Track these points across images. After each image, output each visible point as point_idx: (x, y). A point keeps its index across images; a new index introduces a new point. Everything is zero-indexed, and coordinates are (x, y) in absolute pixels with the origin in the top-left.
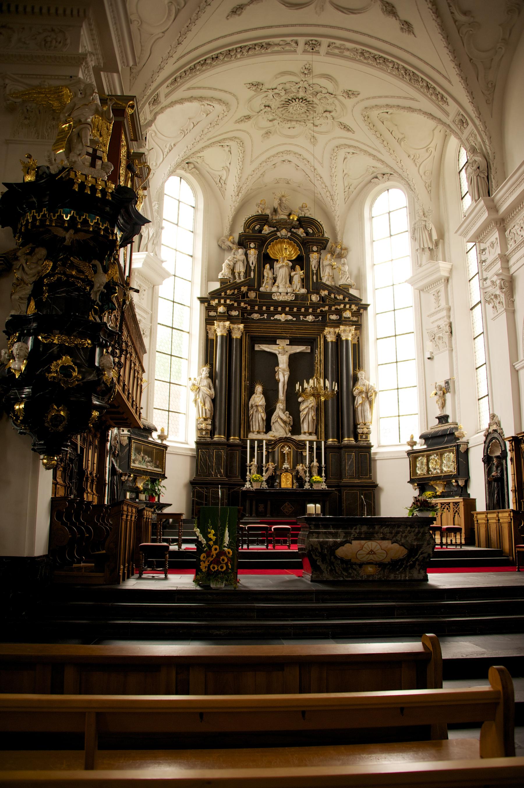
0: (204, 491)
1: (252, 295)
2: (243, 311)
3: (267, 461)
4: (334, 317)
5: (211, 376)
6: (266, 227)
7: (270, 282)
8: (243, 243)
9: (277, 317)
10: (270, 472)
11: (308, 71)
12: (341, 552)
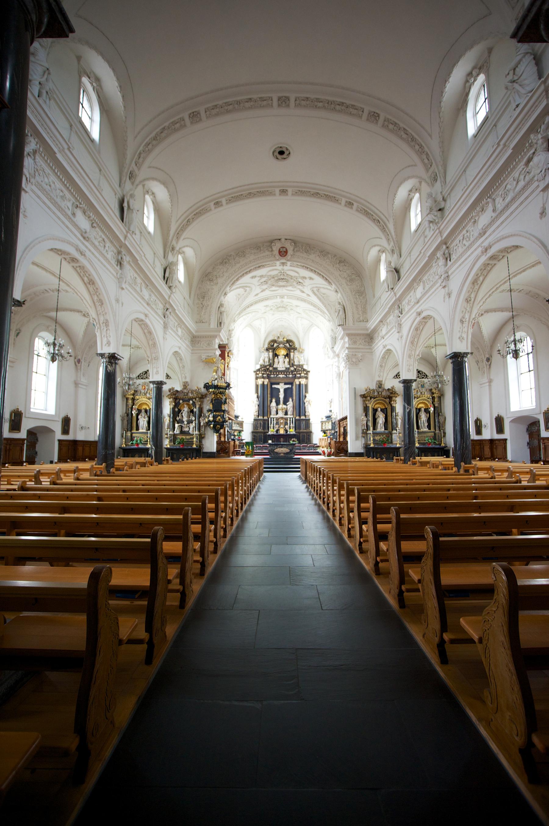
0: (256, 435)
1: (271, 369)
2: (268, 374)
3: (276, 425)
4: (298, 375)
5: (258, 397)
6: (275, 344)
7: (277, 363)
8: (267, 350)
9: (279, 376)
10: (277, 429)
11: (283, 301)
12: (275, 451)
